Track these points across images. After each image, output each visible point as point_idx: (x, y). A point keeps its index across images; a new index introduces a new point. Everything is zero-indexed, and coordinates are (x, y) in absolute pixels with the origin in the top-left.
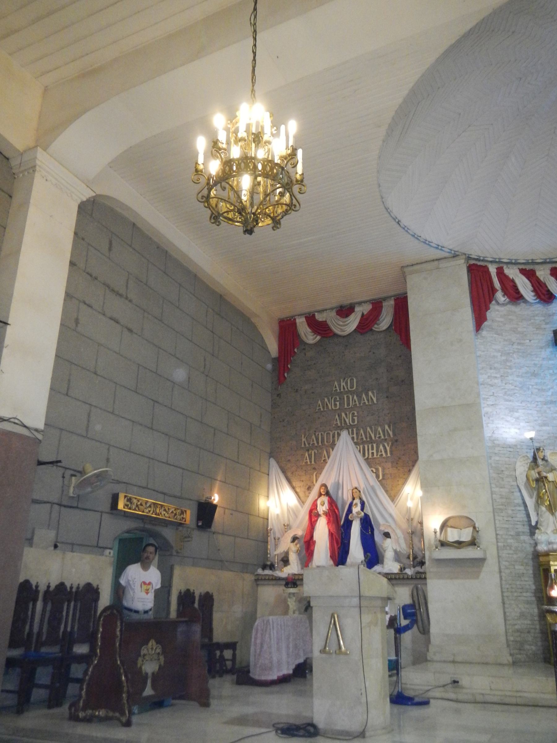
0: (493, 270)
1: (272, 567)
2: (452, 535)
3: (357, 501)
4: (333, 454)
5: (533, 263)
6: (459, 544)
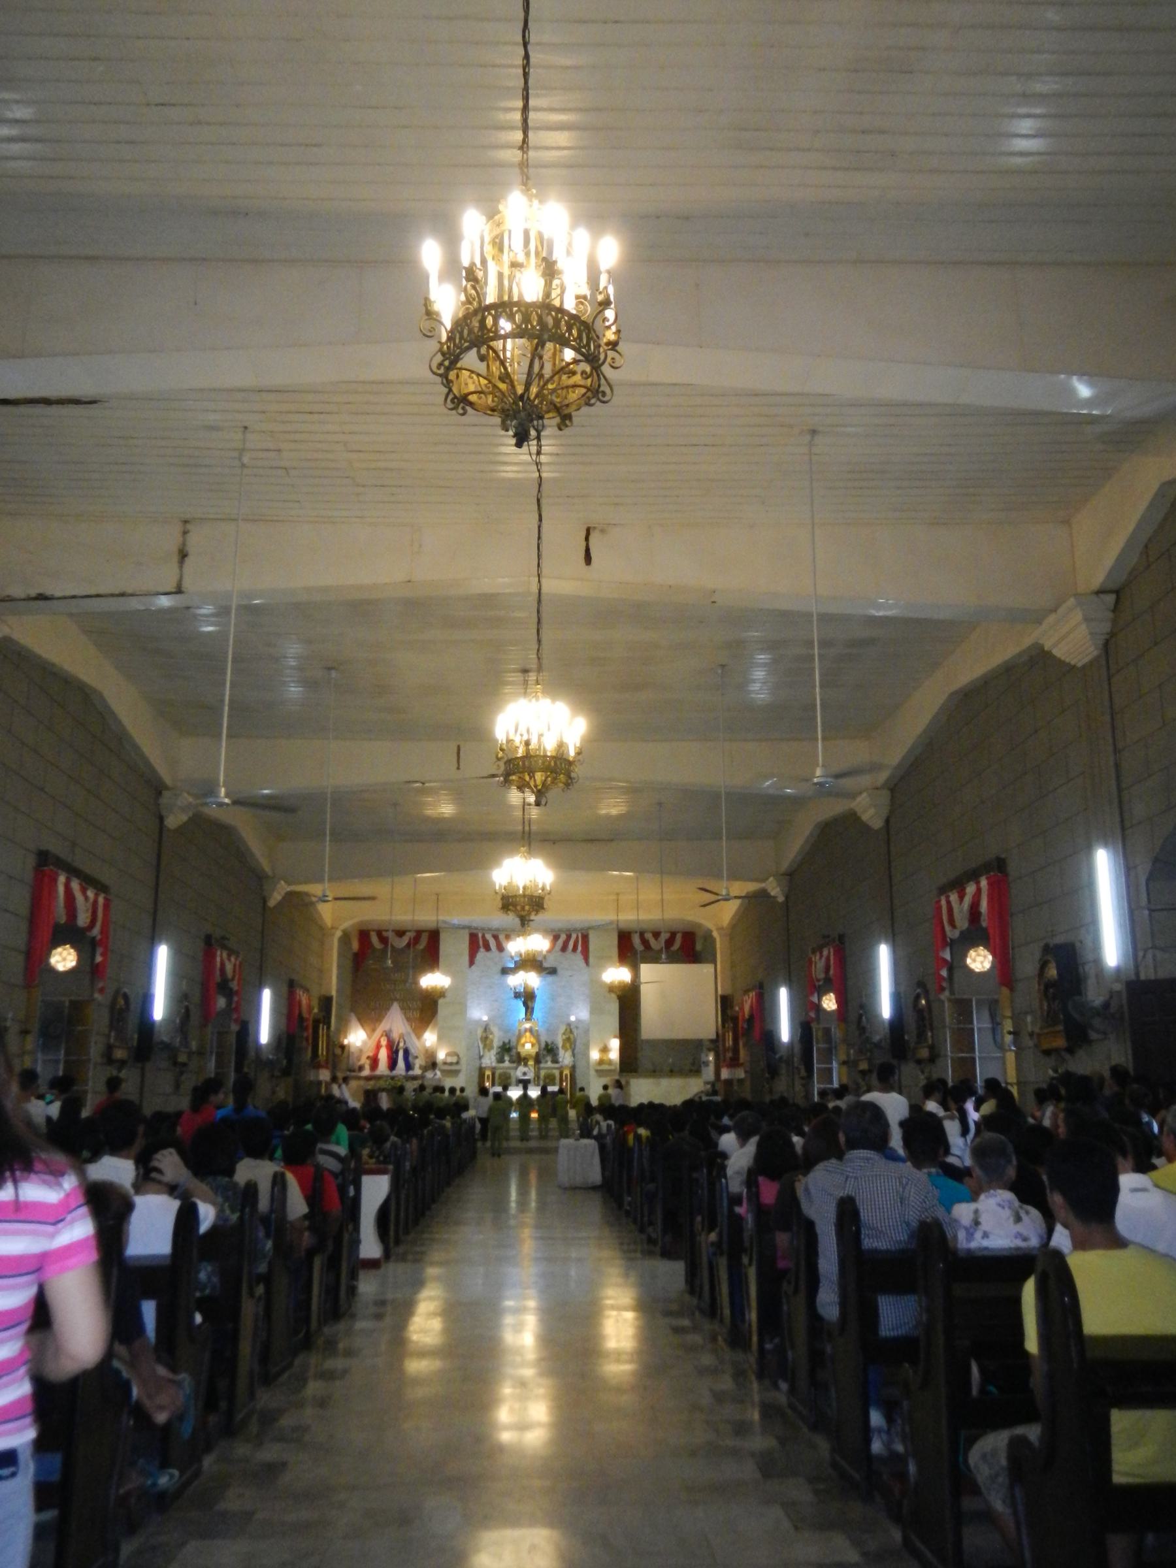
0: (480, 935)
1: (354, 1071)
2: (449, 1060)
3: (402, 1040)
4: (388, 1014)
5: (498, 930)
6: (451, 1064)
